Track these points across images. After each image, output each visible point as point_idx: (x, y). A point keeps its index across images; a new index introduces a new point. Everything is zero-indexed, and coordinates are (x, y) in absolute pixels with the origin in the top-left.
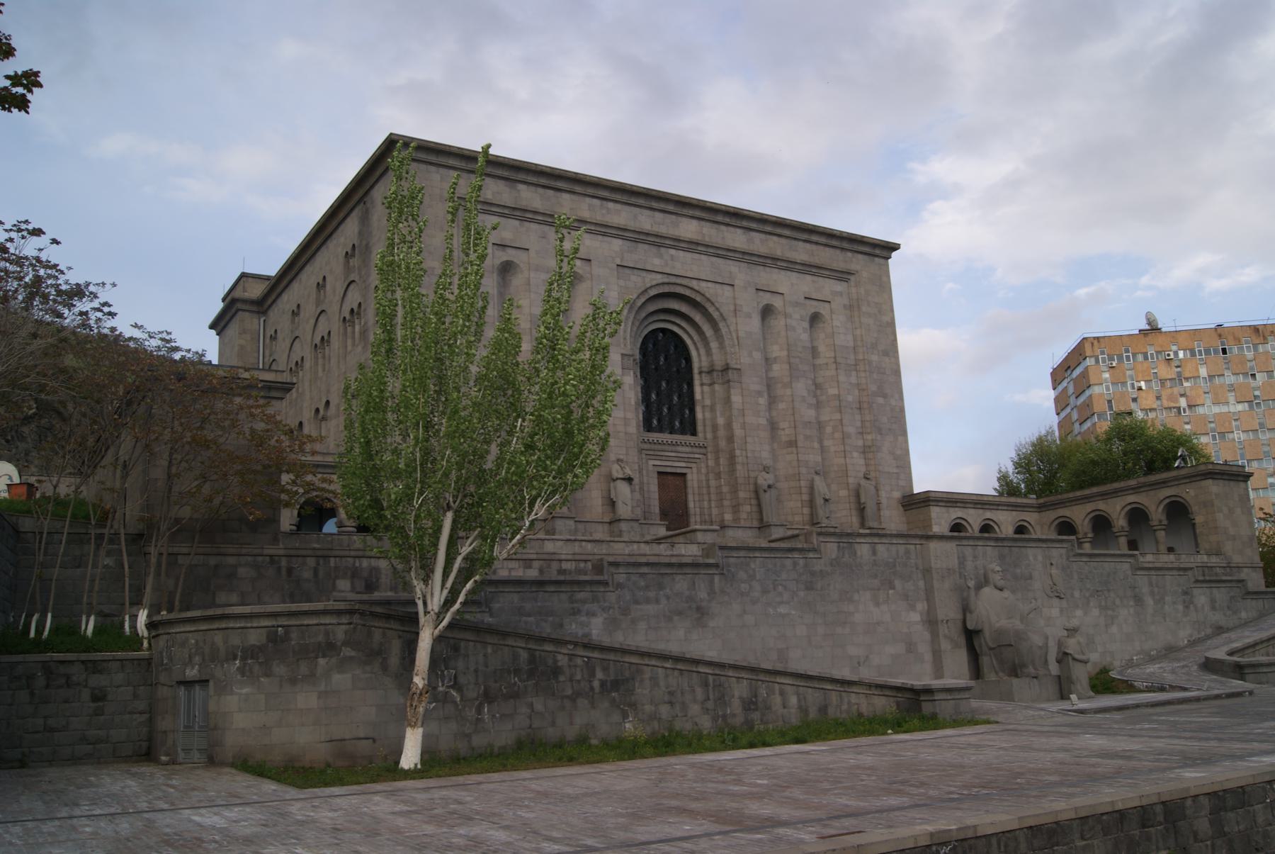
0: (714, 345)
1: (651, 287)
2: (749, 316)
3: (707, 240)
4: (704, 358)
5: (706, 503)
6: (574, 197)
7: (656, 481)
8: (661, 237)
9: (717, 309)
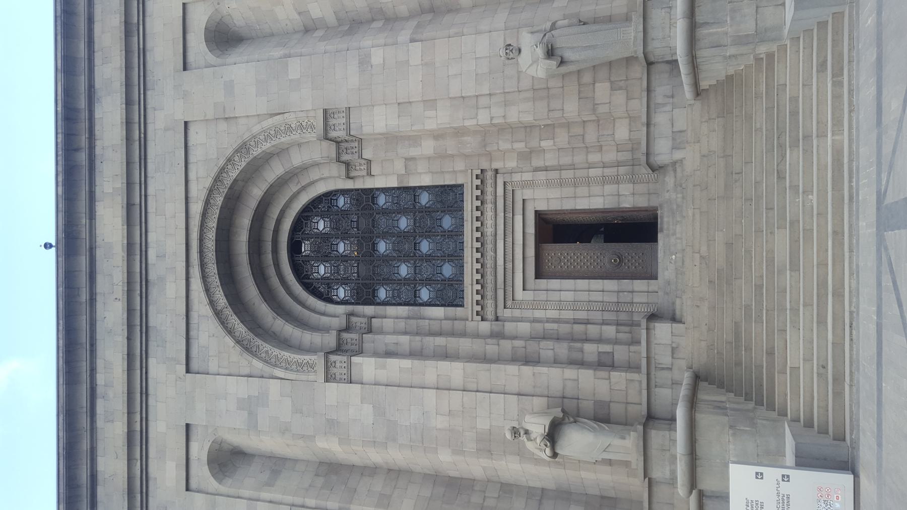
0: (297, 159)
1: (212, 303)
2: (229, 87)
3: (120, 183)
4: (325, 172)
5: (593, 172)
6: (100, 451)
7: (555, 283)
8: (129, 283)
9: (229, 160)
